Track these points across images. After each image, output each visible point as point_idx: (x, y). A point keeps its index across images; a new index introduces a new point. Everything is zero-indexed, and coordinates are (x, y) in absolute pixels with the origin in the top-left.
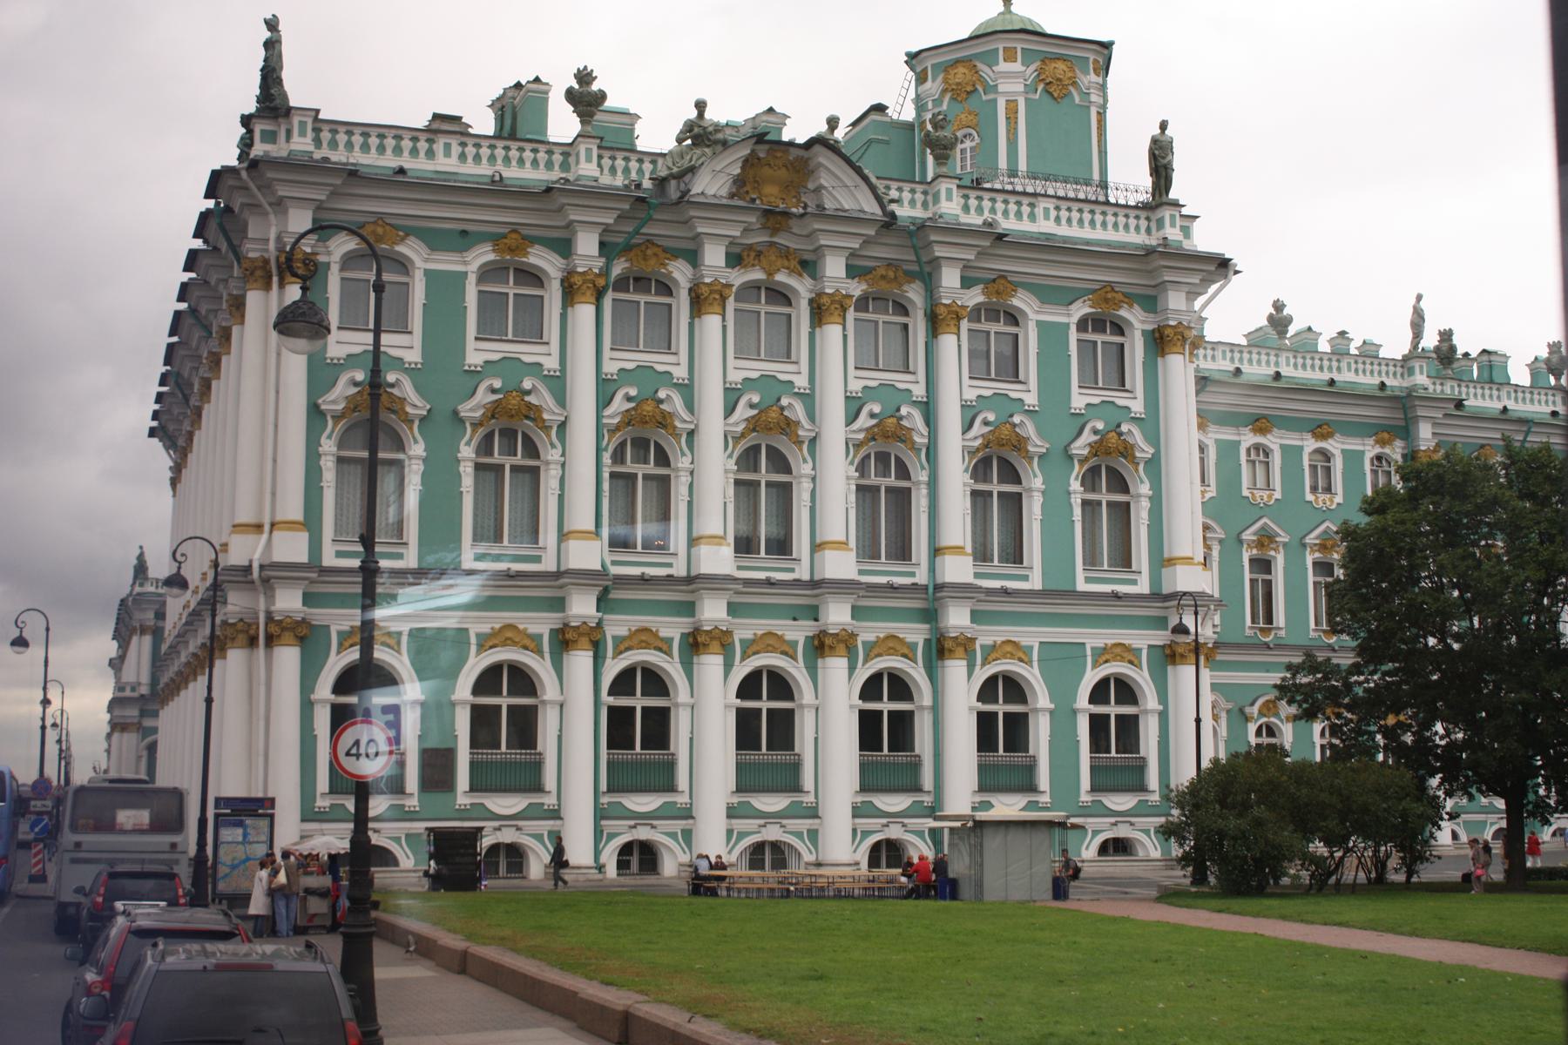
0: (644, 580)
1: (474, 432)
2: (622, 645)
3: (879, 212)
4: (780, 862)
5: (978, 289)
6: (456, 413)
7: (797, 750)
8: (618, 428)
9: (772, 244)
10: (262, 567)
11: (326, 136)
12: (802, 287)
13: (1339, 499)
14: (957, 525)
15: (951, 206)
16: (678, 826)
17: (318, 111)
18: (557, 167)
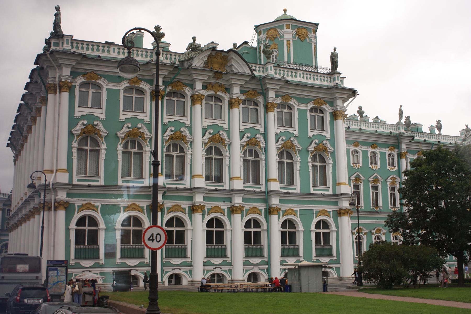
0: (177, 189)
1: (122, 141)
3: (250, 73)
4: (220, 281)
5: (280, 98)
6: (116, 135)
7: (225, 244)
8: (168, 140)
9: (217, 83)
10: (53, 184)
11: (75, 45)
12: (226, 97)
13: (379, 167)
14: (274, 173)
15: (271, 72)
16: (187, 269)
17: (72, 36)
18: (149, 57)
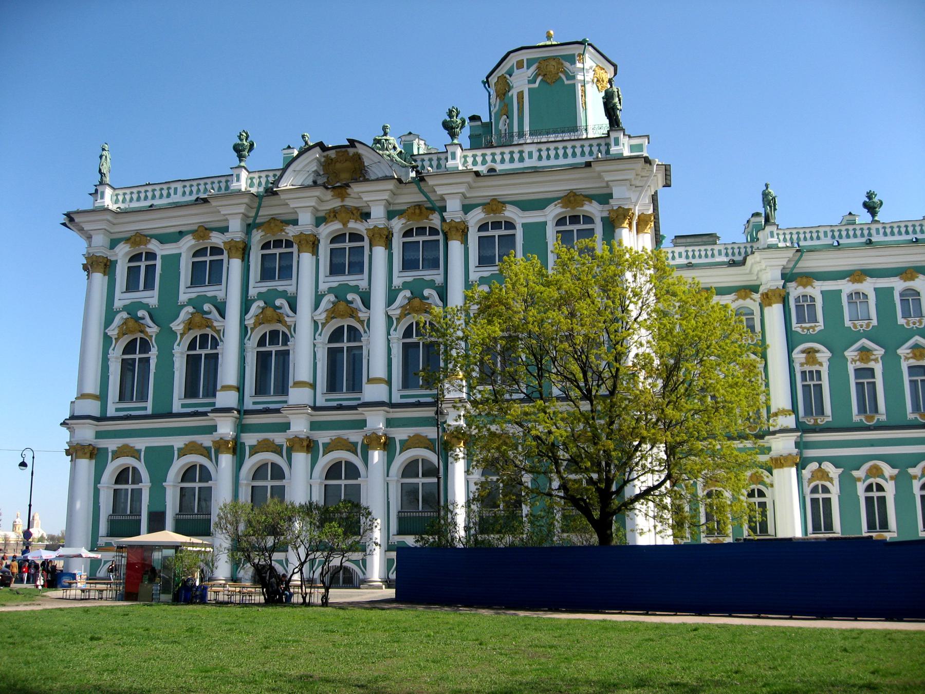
2: (254, 450)
